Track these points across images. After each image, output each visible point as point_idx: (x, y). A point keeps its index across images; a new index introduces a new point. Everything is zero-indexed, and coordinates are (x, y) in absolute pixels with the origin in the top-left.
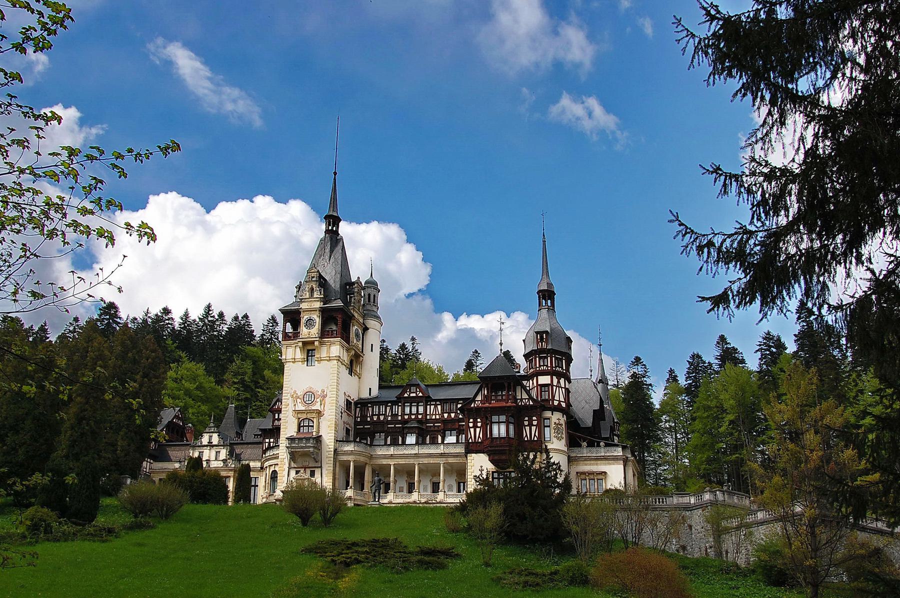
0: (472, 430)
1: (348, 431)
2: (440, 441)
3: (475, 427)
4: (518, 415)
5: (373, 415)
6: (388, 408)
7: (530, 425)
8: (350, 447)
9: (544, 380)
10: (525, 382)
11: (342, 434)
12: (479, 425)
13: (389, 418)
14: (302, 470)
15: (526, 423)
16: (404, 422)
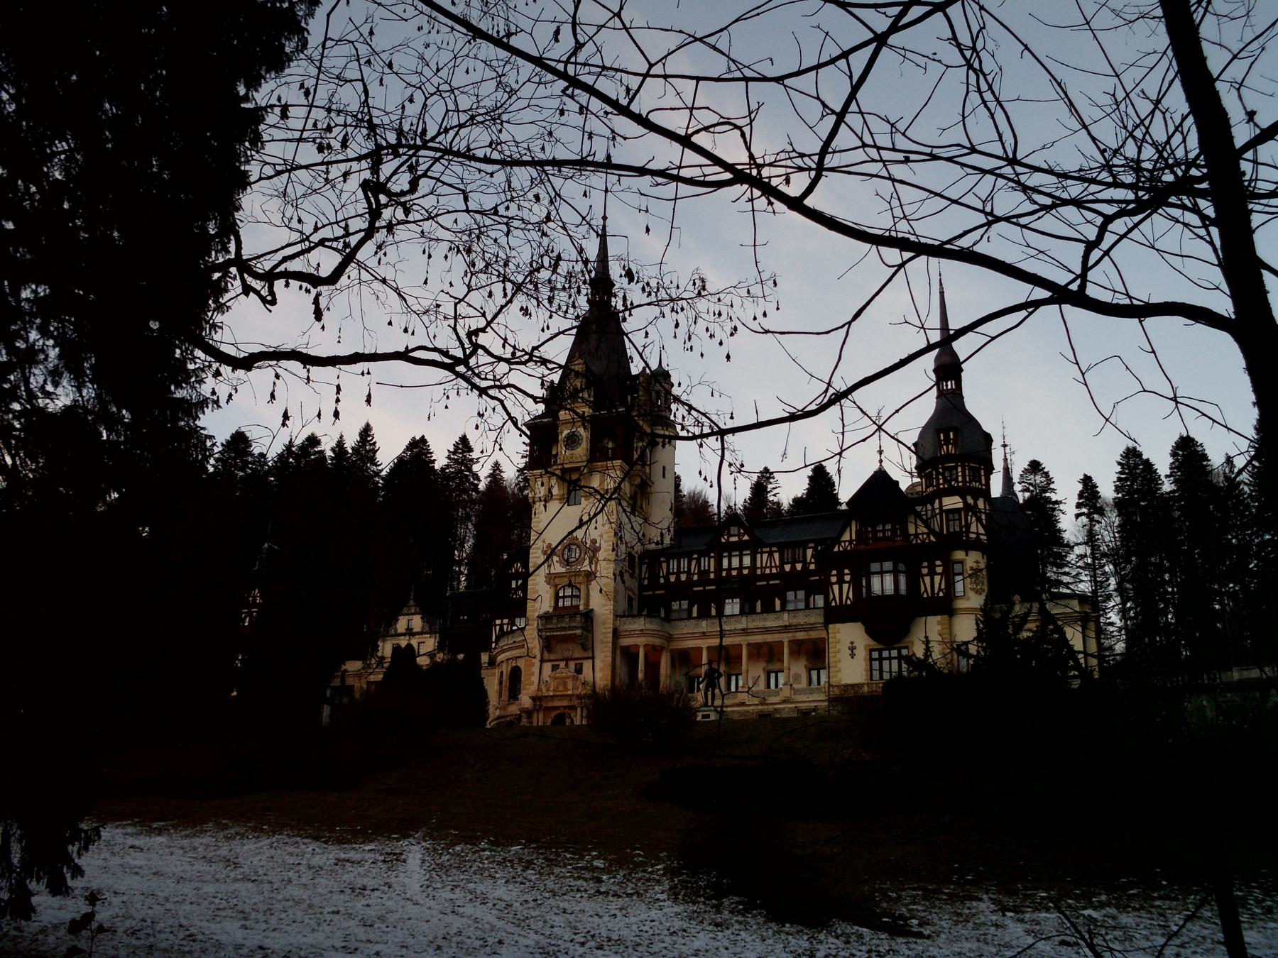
0: (836, 587)
1: (630, 600)
2: (778, 608)
3: (841, 582)
4: (911, 559)
5: (669, 573)
6: (694, 563)
7: (932, 573)
8: (640, 624)
9: (952, 502)
10: (919, 508)
11: (623, 605)
12: (847, 578)
13: (695, 578)
14: (562, 664)
15: (925, 571)
16: (719, 580)
